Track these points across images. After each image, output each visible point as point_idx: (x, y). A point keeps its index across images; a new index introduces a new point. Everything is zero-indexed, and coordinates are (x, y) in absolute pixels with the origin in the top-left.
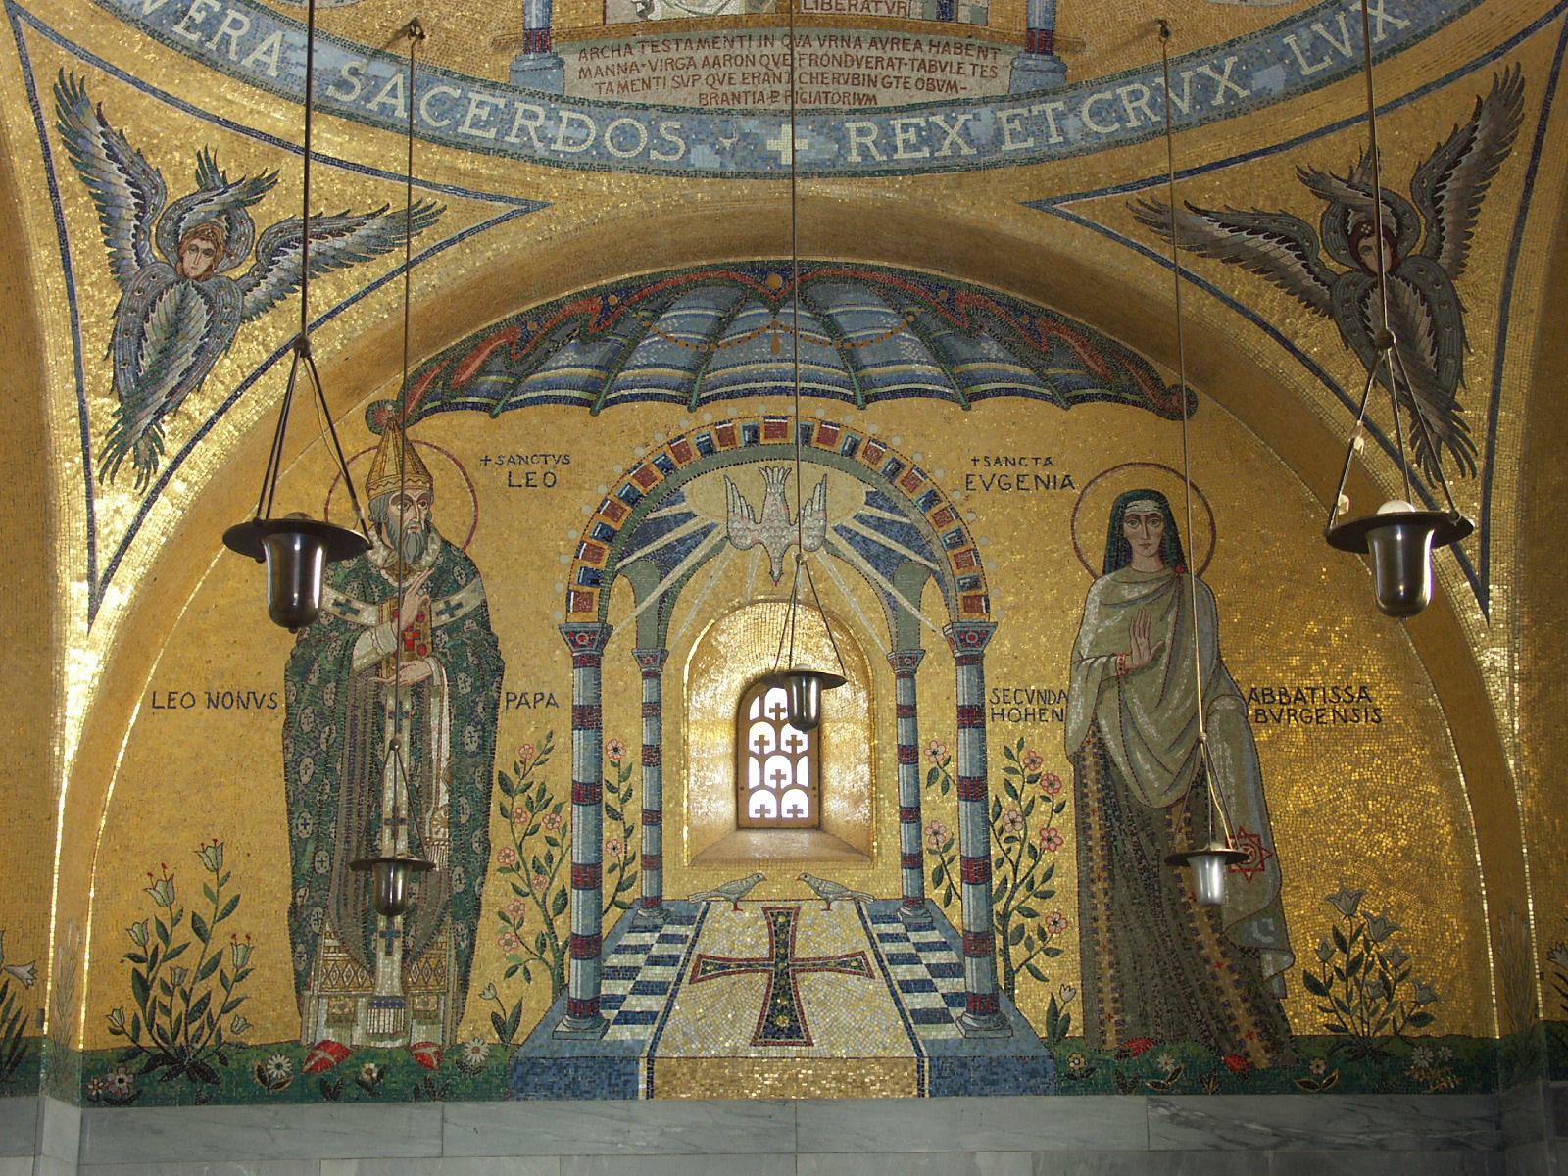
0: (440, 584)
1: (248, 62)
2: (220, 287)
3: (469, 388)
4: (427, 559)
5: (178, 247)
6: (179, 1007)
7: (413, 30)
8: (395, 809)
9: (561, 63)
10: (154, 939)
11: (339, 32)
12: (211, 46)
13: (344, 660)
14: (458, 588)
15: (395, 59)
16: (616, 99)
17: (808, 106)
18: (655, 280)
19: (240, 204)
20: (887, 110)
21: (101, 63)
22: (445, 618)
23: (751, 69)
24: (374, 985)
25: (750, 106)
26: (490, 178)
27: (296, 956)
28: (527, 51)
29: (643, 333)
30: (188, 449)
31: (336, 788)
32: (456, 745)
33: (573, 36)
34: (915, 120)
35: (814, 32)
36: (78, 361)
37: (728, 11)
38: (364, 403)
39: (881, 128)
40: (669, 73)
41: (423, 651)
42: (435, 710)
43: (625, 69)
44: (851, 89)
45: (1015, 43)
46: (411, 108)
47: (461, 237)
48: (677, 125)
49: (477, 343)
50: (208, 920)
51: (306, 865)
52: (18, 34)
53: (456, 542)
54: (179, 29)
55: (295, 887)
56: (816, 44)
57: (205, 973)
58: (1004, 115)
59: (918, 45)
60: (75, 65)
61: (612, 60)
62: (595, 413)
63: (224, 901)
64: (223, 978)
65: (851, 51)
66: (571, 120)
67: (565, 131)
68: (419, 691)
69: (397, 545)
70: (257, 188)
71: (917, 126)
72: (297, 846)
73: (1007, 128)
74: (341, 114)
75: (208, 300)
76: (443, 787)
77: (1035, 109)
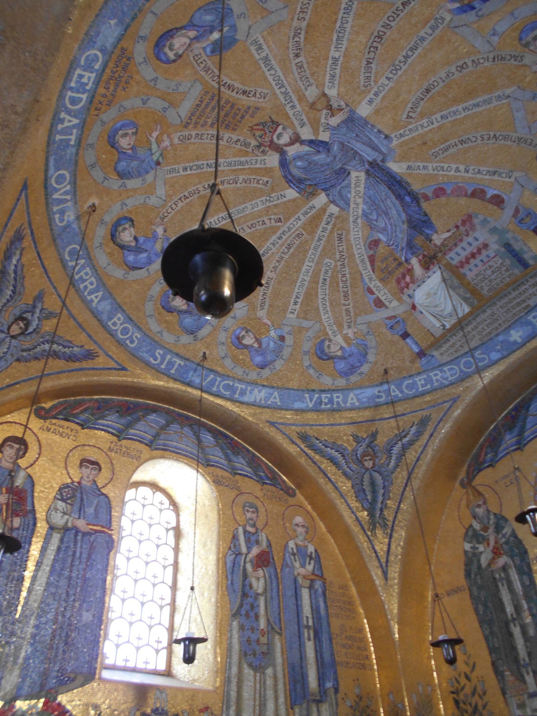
0: (498, 529)
1: (348, 405)
2: (380, 467)
3: (484, 462)
4: (491, 522)
5: (360, 462)
6: (470, 709)
7: (386, 372)
8: (512, 615)
9: (433, 356)
10: (456, 684)
11: (367, 384)
12: (335, 406)
13: (479, 566)
14: (503, 528)
18: (522, 400)
19: (371, 442)
21: (307, 425)
22: (503, 540)
23: (487, 323)
24: (527, 688)
26: (438, 398)
27: (499, 681)
29: (526, 418)
30: (395, 517)
31: (491, 613)
32: (523, 584)
36: (348, 505)
38: (458, 481)
41: (500, 554)
42: (511, 574)
43: (452, 346)
44: (520, 308)
46: (402, 392)
47: (441, 419)
48: (480, 352)
49: (481, 448)
50: (468, 673)
51: (491, 645)
52: (278, 429)
53: (497, 512)
54: (323, 406)
55: (490, 654)
57: (473, 694)
59: (527, 281)
60: (299, 429)
61: (446, 346)
62: (522, 450)
63: (471, 664)
64: (479, 695)
65: (510, 297)
66: (449, 370)
67: (449, 374)
68: (504, 568)
69: (481, 522)
70: (374, 436)
72: (486, 638)
74: (384, 404)
75: (378, 472)
76: (524, 602)
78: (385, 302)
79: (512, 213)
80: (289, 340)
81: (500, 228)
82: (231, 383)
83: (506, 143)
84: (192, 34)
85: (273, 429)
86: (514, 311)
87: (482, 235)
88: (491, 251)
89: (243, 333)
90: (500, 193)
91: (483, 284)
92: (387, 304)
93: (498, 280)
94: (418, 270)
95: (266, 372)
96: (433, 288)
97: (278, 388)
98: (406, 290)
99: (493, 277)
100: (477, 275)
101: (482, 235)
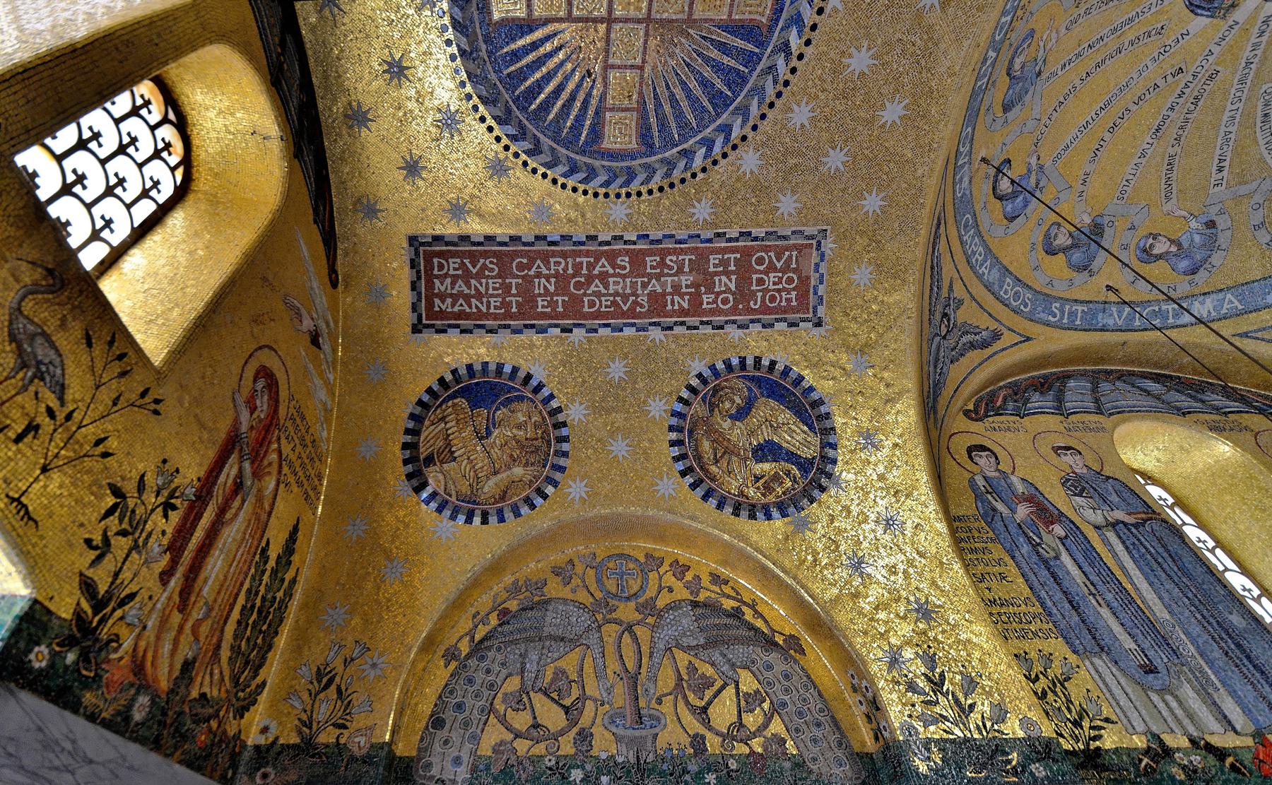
52: (1257, 338)
80: (1222, 222)
82: (1157, 309)
85: (1246, 341)
89: (1151, 241)
95: (1202, 275)
97: (1229, 289)
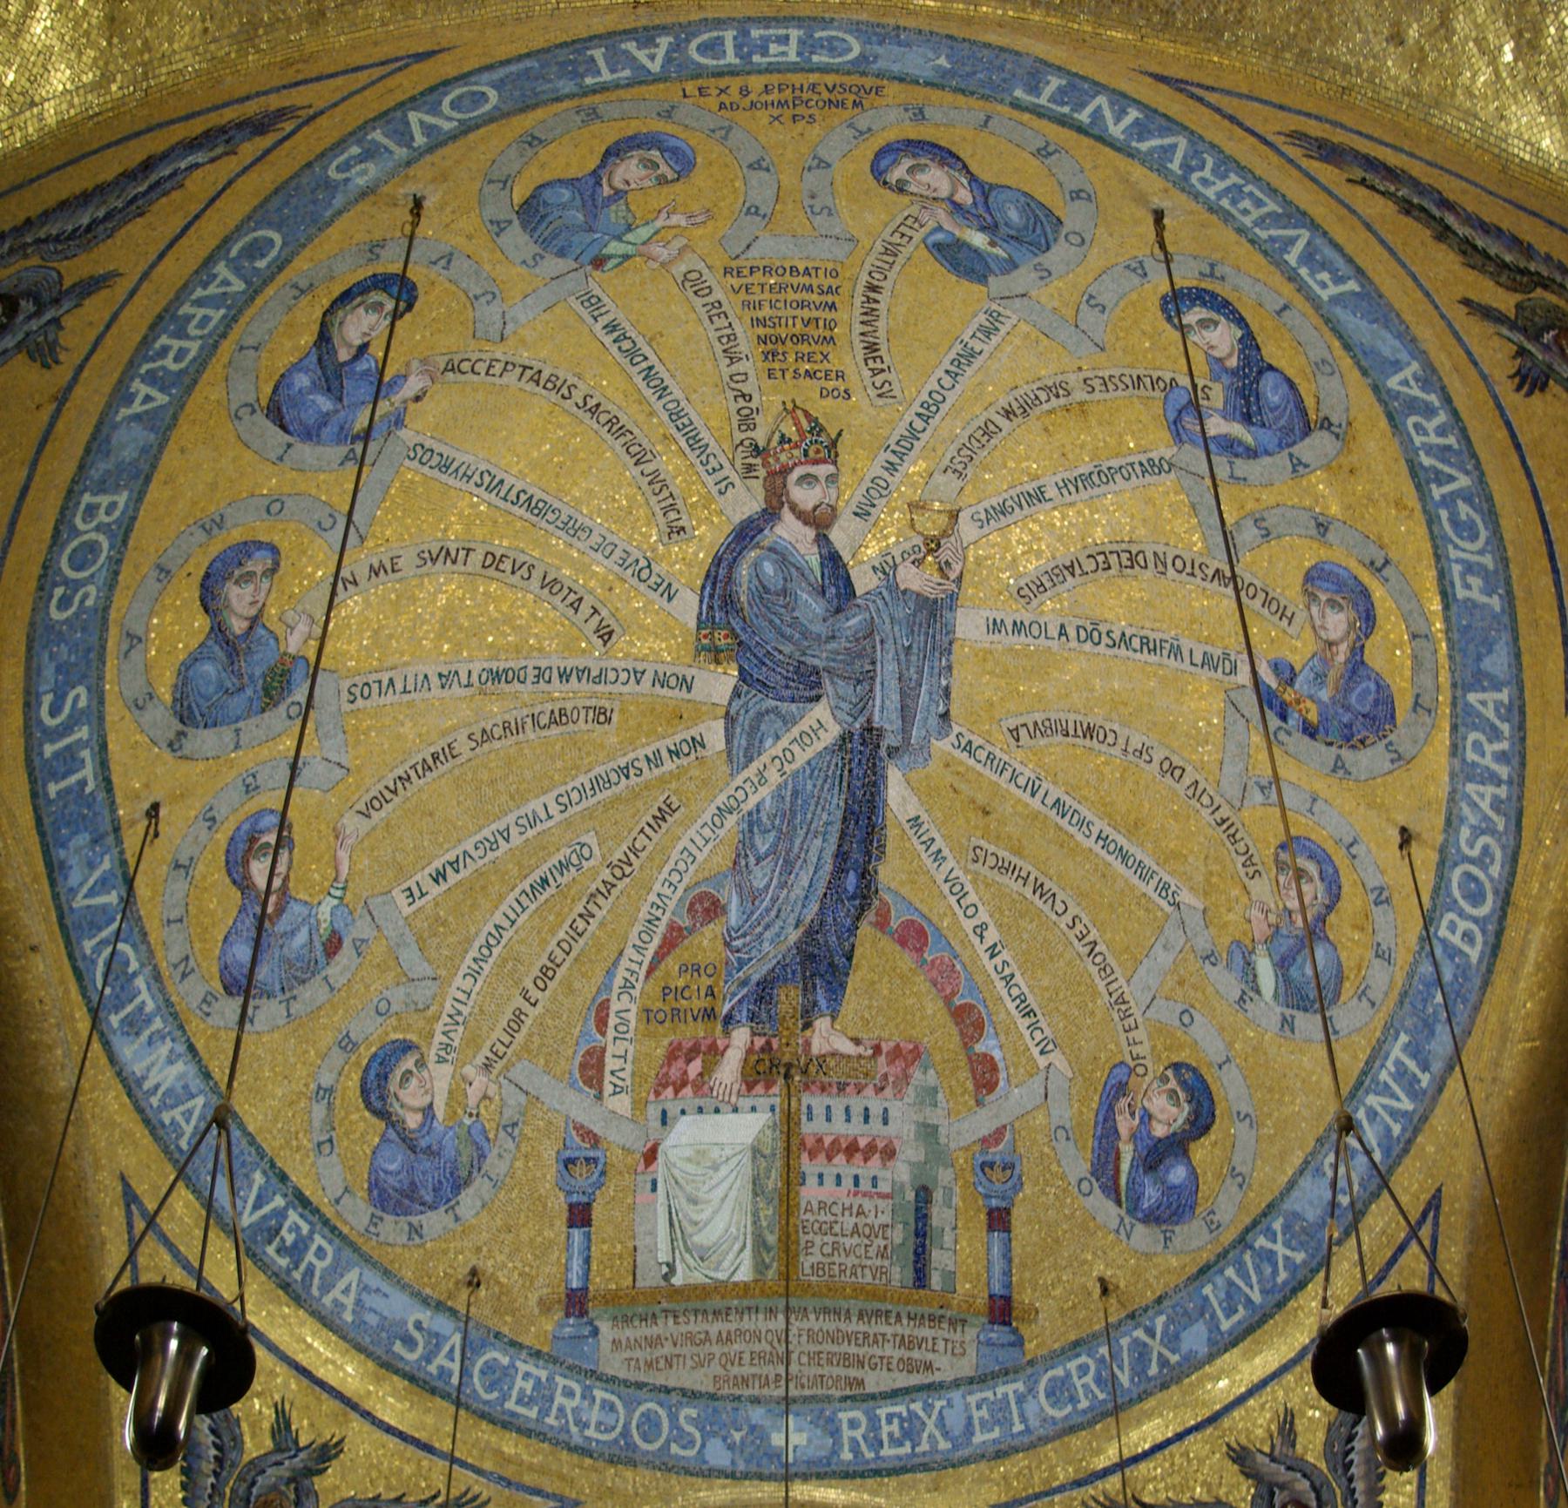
15: (453, 1312)
16: (642, 1378)
17: (807, 1392)
20: (873, 1397)
25: (756, 1392)
28: (568, 1315)
33: (611, 1299)
34: (897, 1409)
35: (811, 1303)
37: (737, 1278)
39: (870, 1419)
40: (687, 1350)
45: (977, 1314)
56: (812, 1317)
58: (973, 1399)
65: (843, 1326)
71: (899, 1416)
73: (976, 1415)
77: (1000, 1390)
78: (608, 1078)
79: (985, 1132)
81: (943, 1140)
83: (1097, 980)
84: (964, 196)
86: (826, 1370)
87: (901, 1119)
88: (888, 1175)
90: (1001, 1065)
91: (818, 1240)
92: (608, 1089)
93: (851, 1261)
94: (729, 1070)
96: (721, 1146)
98: (670, 1091)
99: (848, 1242)
100: (822, 1206)
101: (902, 1123)
